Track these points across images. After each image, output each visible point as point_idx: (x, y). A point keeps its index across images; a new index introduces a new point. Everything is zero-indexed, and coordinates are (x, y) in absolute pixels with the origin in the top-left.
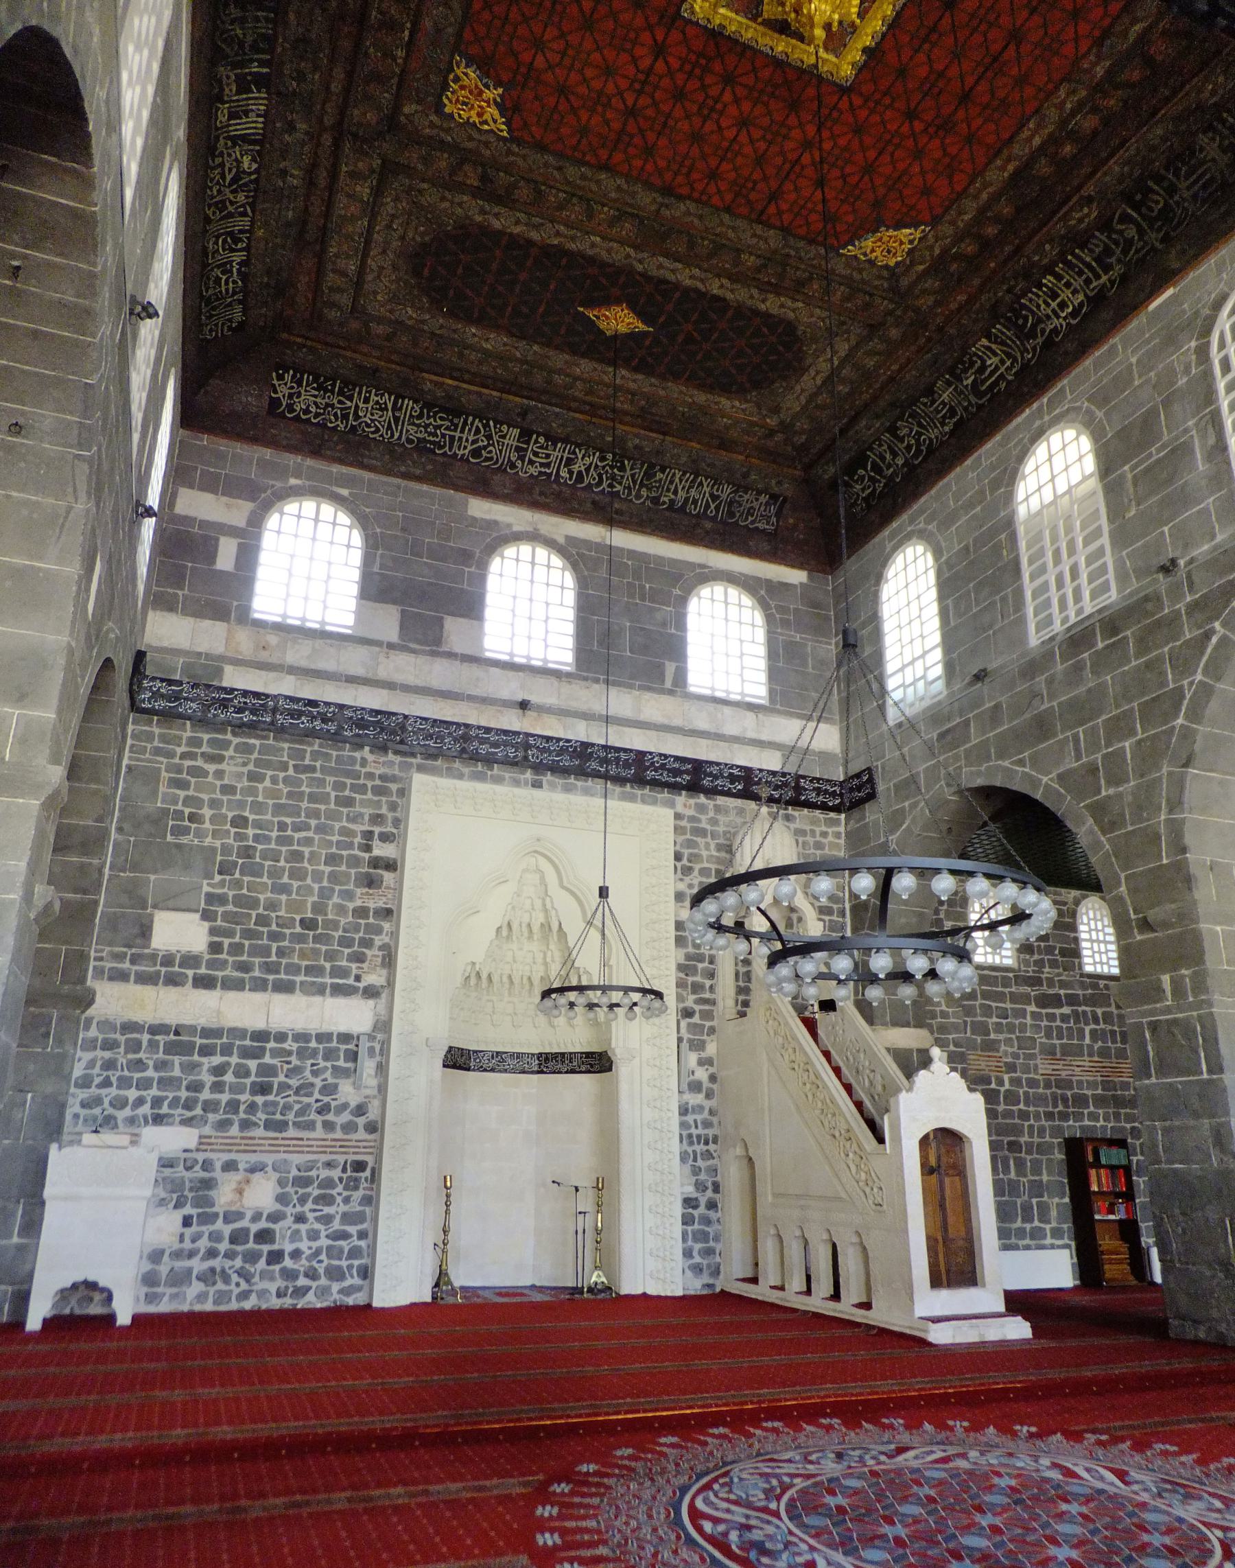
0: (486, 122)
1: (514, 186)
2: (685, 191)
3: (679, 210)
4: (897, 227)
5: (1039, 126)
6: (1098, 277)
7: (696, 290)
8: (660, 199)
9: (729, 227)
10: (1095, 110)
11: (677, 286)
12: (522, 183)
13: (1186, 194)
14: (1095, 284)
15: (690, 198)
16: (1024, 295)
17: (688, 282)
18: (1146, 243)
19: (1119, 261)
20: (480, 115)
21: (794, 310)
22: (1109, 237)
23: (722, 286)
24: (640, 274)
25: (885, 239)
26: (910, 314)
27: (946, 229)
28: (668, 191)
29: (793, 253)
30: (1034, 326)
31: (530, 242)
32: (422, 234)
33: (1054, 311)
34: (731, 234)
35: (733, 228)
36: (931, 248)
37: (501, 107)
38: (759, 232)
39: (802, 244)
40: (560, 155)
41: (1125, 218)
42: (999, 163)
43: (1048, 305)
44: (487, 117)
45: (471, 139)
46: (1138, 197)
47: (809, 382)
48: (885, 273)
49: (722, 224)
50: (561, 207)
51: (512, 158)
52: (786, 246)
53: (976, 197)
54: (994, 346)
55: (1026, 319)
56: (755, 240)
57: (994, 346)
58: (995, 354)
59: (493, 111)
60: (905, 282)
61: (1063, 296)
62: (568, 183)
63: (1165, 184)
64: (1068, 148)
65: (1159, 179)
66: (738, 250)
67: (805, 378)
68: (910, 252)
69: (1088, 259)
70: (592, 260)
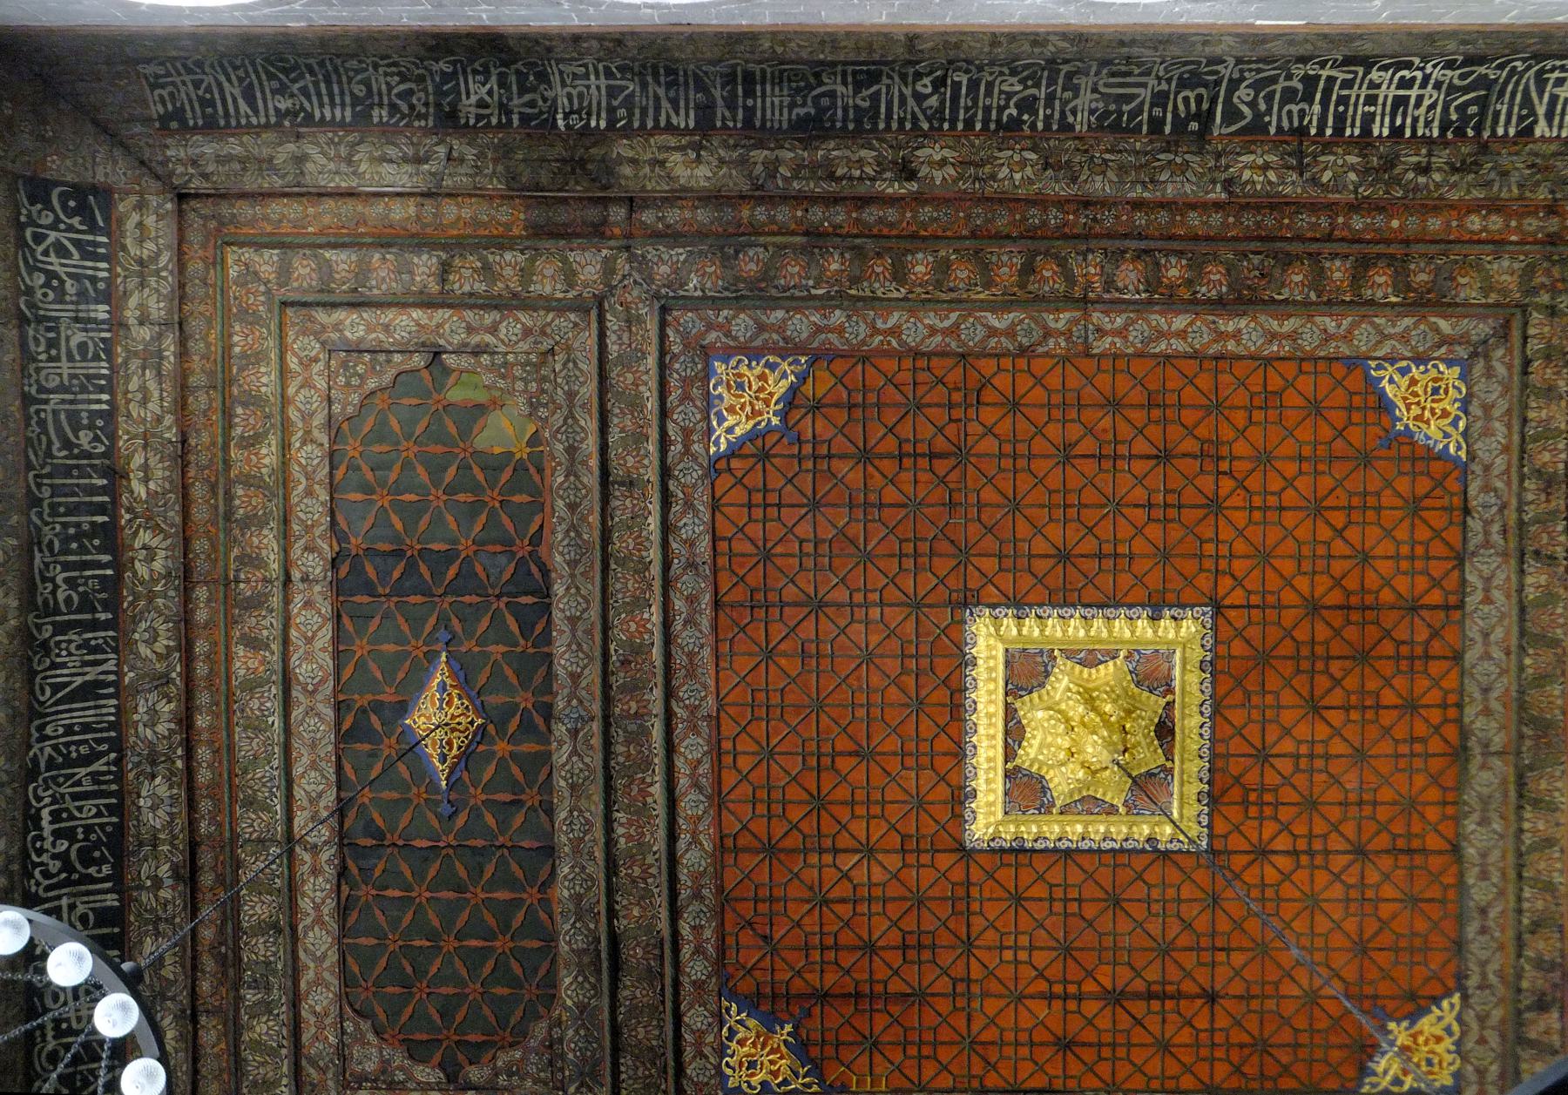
0: (1448, 1030)
2: (1451, 732)
3: (1488, 726)
4: (1384, 406)
5: (1161, 334)
6: (1331, 80)
8: (1478, 760)
9: (1486, 643)
10: (1109, 284)
12: (1530, 953)
13: (1152, 82)
14: (1342, 76)
15: (1459, 721)
16: (1428, 141)
18: (1242, 71)
19: (1289, 77)
20: (1439, 1040)
22: (1269, 111)
25: (1415, 410)
26: (1540, 279)
27: (1363, 338)
28: (1459, 753)
29: (1496, 528)
30: (1465, 90)
33: (1423, 86)
34: (1498, 634)
35: (1486, 635)
36: (1404, 338)
37: (1413, 1017)
38: (1479, 595)
39: (1475, 524)
40: (1461, 920)
41: (1232, 115)
42: (1231, 346)
43: (1420, 99)
44: (1438, 1031)
45: (1482, 1041)
46: (1194, 126)
48: (1479, 368)
51: (1492, 978)
52: (1487, 544)
53: (1293, 336)
54: (1541, 110)
55: (1461, 109)
56: (1497, 595)
57: (1541, 110)
58: (1554, 99)
59: (1426, 1024)
60: (1481, 329)
61: (1393, 92)
62: (1502, 893)
63: (1157, 111)
64: (1173, 272)
65: (1156, 125)
66: (1522, 610)
68: (1420, 359)
69: (1317, 108)
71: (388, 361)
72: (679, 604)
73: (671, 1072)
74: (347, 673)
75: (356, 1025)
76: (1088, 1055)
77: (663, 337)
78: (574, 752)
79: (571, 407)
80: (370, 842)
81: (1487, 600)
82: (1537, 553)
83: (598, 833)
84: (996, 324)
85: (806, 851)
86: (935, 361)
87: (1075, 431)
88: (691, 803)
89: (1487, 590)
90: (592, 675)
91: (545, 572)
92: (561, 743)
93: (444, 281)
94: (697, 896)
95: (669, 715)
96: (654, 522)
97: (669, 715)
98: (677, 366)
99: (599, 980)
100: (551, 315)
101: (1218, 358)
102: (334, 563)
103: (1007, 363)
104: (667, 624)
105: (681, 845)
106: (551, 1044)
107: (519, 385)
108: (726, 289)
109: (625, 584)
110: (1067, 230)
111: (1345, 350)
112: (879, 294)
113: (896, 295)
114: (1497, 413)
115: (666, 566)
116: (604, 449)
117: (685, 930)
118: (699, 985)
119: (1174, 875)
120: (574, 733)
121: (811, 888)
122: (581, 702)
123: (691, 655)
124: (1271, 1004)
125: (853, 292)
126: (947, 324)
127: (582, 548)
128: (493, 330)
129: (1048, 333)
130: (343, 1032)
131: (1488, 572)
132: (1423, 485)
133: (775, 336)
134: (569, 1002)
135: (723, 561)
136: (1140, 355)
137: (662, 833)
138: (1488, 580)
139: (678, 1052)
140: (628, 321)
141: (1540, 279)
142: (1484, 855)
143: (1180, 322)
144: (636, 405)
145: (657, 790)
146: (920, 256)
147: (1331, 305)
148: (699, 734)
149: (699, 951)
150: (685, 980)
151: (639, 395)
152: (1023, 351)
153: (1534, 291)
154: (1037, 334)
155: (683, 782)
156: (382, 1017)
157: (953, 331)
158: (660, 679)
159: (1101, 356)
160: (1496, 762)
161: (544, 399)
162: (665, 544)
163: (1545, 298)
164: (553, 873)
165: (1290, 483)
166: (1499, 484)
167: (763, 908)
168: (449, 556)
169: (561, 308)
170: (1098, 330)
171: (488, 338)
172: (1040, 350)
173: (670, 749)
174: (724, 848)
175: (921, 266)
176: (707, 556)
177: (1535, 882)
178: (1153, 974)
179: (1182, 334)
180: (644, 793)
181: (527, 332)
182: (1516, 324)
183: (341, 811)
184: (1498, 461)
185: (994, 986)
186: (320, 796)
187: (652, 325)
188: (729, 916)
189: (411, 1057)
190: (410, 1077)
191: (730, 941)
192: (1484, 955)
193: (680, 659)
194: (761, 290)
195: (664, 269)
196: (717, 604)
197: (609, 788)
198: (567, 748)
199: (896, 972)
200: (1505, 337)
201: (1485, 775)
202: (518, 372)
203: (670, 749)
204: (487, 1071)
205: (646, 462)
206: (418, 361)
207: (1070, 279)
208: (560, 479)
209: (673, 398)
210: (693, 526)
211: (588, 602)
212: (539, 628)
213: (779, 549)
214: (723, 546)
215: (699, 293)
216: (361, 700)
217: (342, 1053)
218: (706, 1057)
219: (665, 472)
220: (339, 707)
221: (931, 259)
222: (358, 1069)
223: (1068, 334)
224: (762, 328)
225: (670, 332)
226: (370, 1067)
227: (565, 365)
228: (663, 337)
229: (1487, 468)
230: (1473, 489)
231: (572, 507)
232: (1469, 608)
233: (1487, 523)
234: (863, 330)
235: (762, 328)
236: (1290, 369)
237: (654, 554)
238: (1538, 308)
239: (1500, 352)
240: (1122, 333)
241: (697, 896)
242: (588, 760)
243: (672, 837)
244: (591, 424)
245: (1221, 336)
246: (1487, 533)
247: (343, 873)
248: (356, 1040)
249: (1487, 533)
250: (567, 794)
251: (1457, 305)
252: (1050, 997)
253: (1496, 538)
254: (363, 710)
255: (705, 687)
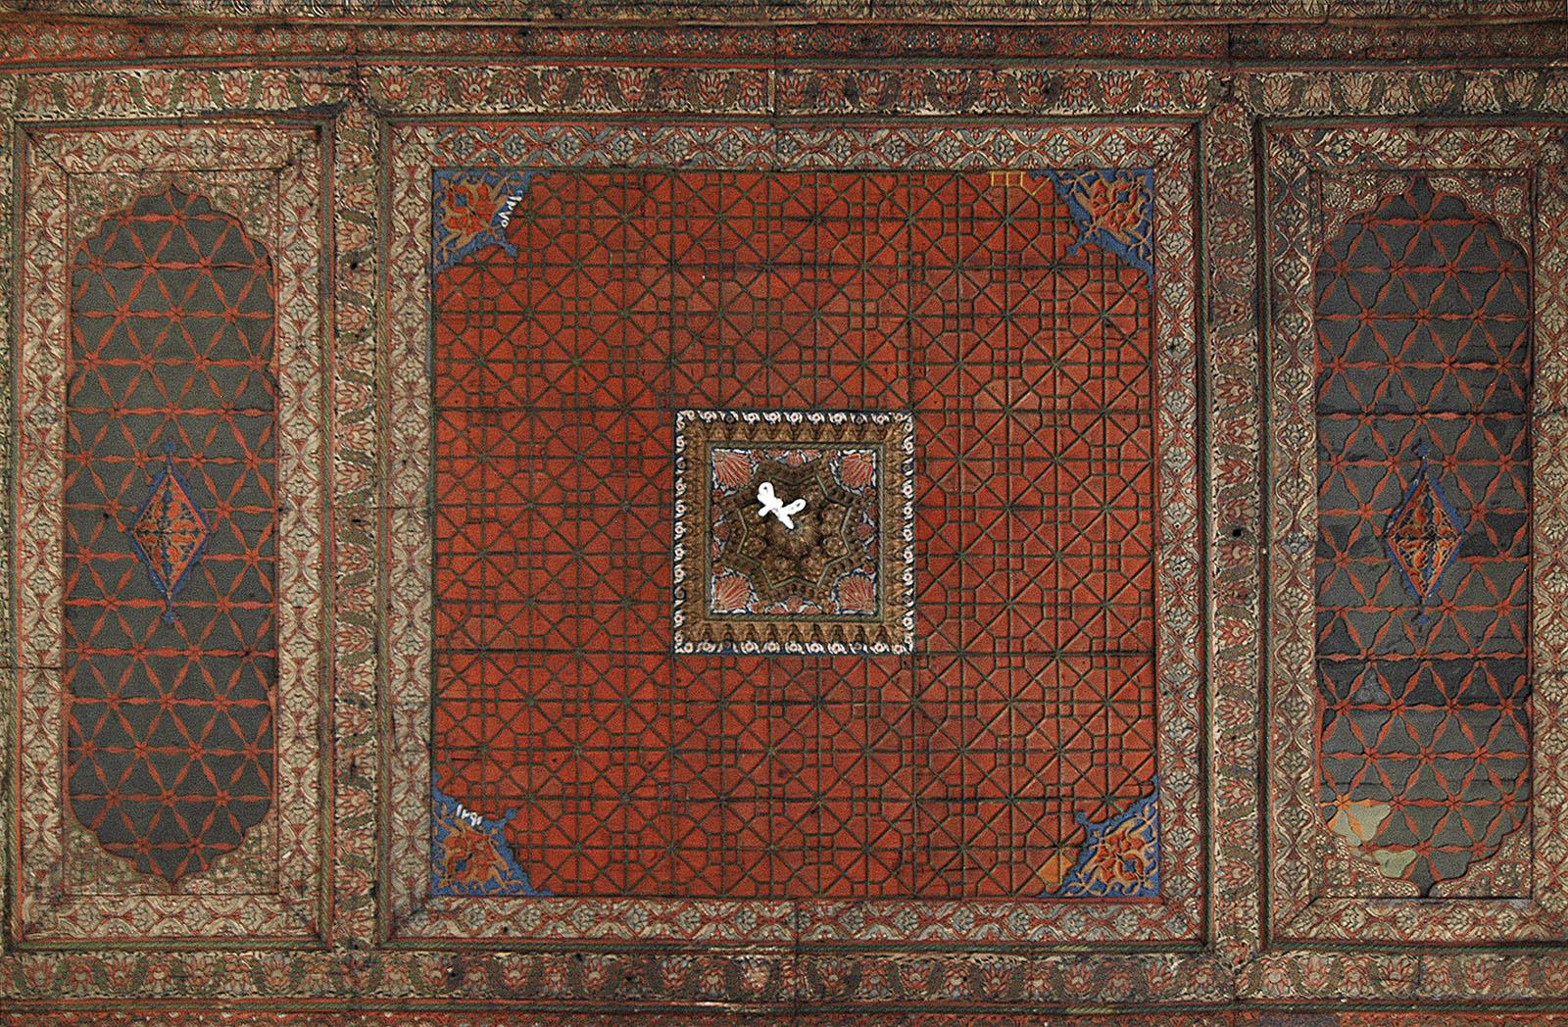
1: (357, 300)
3: (410, 539)
7: (275, 628)
9: (410, 616)
11: (274, 595)
15: (436, 540)
17: (287, 609)
21: (299, 795)
23: (299, 662)
24: (274, 531)
28: (435, 510)
29: (402, 730)
31: (271, 351)
32: (224, 196)
35: (410, 624)
38: (418, 664)
39: (422, 733)
42: (658, 910)
47: (151, 913)
49: (410, 605)
50: (347, 375)
52: (411, 714)
53: (598, 919)
56: (402, 665)
60: (420, 926)
64: (713, 980)
67: (156, 902)
70: (276, 452)
71: (1472, 888)
72: (1191, 655)
73: (1204, 191)
74: (1519, 583)
75: (1518, 232)
76: (792, 208)
77: (1205, 914)
78: (1295, 509)
79: (1294, 845)
80: (1501, 416)
81: (410, 659)
82: (363, 704)
83: (1275, 428)
84: (883, 928)
85: (1068, 411)
86: (943, 892)
87: (809, 826)
88: (1180, 458)
89: (411, 669)
90: (1278, 586)
91: (1321, 688)
92: (1308, 517)
93: (1420, 970)
94: (1176, 367)
95: (1203, 546)
96: (1215, 733)
97: (1203, 546)
98: (1191, 885)
99: (1273, 281)
100: (1313, 934)
101: (671, 897)
102: (1529, 691)
103: (874, 890)
104: (1203, 635)
105: (1190, 417)
106: (1321, 218)
107: (1344, 866)
108: (1143, 960)
109: (1245, 672)
110: (814, 1020)
111: (549, 906)
112: (996, 958)
113: (979, 956)
114: (403, 844)
115: (1203, 691)
116: (1263, 806)
117: (1188, 333)
118: (1176, 278)
119: (709, 385)
120: (1296, 528)
121: (1063, 374)
122: (1289, 558)
123: (1179, 604)
124: (614, 258)
125: (1021, 959)
126: (931, 929)
127: (1285, 710)
128: (1370, 920)
129: (834, 920)
130: (1531, 227)
131: (412, 691)
132: (471, 773)
133: (1096, 915)
134: (1304, 259)
135: (1145, 695)
136: (746, 899)
137: (1212, 427)
138: (410, 679)
139: (1196, 208)
140: (1237, 929)
141: (364, 976)
142: (411, 406)
143: (707, 931)
144: (1230, 849)
145: (1215, 472)
146: (956, 994)
147: (560, 946)
148: (1172, 526)
149: (1175, 312)
150: (1189, 282)
151: (1228, 856)
152: (858, 904)
153: (367, 963)
154: (844, 918)
155: (1188, 479)
156: (1492, 242)
157: (924, 922)
158: (1211, 581)
159: (781, 898)
160: (398, 499)
161: (1319, 853)
162: (1204, 712)
163: (359, 956)
164: (1318, 388)
165: (601, 774)
166: (399, 773)
167: (1111, 356)
168: (1415, 699)
169: (1300, 942)
170: (785, 924)
171: (1374, 912)
172: (841, 905)
173: (1201, 512)
174: (1148, 414)
175: (955, 986)
176: (1162, 700)
177: (362, 379)
178: (732, 288)
179: (705, 920)
180: (1227, 468)
181: (1337, 918)
182: (385, 931)
183: (1528, 451)
184: (401, 796)
185: (885, 277)
186: (1550, 462)
187: (1216, 925)
188: (1144, 349)
189: (1463, 202)
190: (1463, 181)
191: (1143, 322)
192: (410, 307)
193: (1190, 602)
194: (1109, 960)
195: (1202, 979)
196: (1153, 654)
197: (1264, 472)
198: (1303, 511)
199: (981, 291)
200: (395, 917)
201: (411, 487)
202: (1346, 879)
203: (1201, 512)
204: (1386, 189)
205: (1221, 792)
206: (1443, 889)
207: (812, 974)
208: (1306, 775)
209: (1195, 853)
210: (1177, 729)
211: (1280, 656)
212: (1328, 630)
213: (1093, 707)
214: (1146, 709)
215: (1169, 956)
216: (1508, 557)
217: (1533, 203)
218: (1168, 204)
219: (1203, 781)
220: (1529, 549)
221: (946, 991)
222: (1516, 190)
223: (814, 920)
224: (1109, 923)
225: (1197, 918)
226: (1504, 192)
227: (1300, 886)
228: (1205, 914)
229: (411, 789)
230: (426, 765)
231: (1293, 748)
232: (428, 650)
233: (411, 735)
234: (1011, 921)
235: (1109, 923)
236: (600, 885)
237: (1216, 702)
238: (365, 948)
239: (400, 902)
240: (762, 921)
241: (1176, 367)
242: (1282, 501)
243: (1200, 424)
244: (1277, 829)
245: (668, 919)
246: (411, 725)
247: (1528, 385)
248: (1518, 218)
249: (411, 725)
250: (1304, 467)
251: (443, 950)
252: (831, 264)
253: (402, 720)
254: (1505, 547)
255: (1165, 573)
